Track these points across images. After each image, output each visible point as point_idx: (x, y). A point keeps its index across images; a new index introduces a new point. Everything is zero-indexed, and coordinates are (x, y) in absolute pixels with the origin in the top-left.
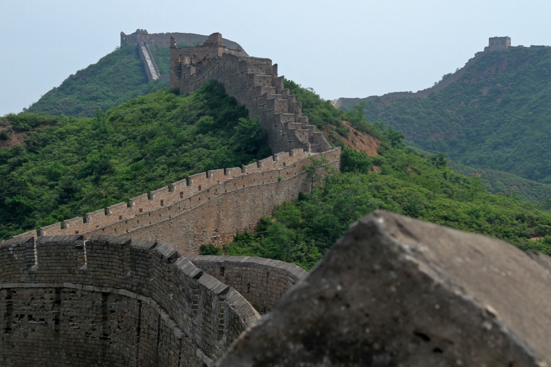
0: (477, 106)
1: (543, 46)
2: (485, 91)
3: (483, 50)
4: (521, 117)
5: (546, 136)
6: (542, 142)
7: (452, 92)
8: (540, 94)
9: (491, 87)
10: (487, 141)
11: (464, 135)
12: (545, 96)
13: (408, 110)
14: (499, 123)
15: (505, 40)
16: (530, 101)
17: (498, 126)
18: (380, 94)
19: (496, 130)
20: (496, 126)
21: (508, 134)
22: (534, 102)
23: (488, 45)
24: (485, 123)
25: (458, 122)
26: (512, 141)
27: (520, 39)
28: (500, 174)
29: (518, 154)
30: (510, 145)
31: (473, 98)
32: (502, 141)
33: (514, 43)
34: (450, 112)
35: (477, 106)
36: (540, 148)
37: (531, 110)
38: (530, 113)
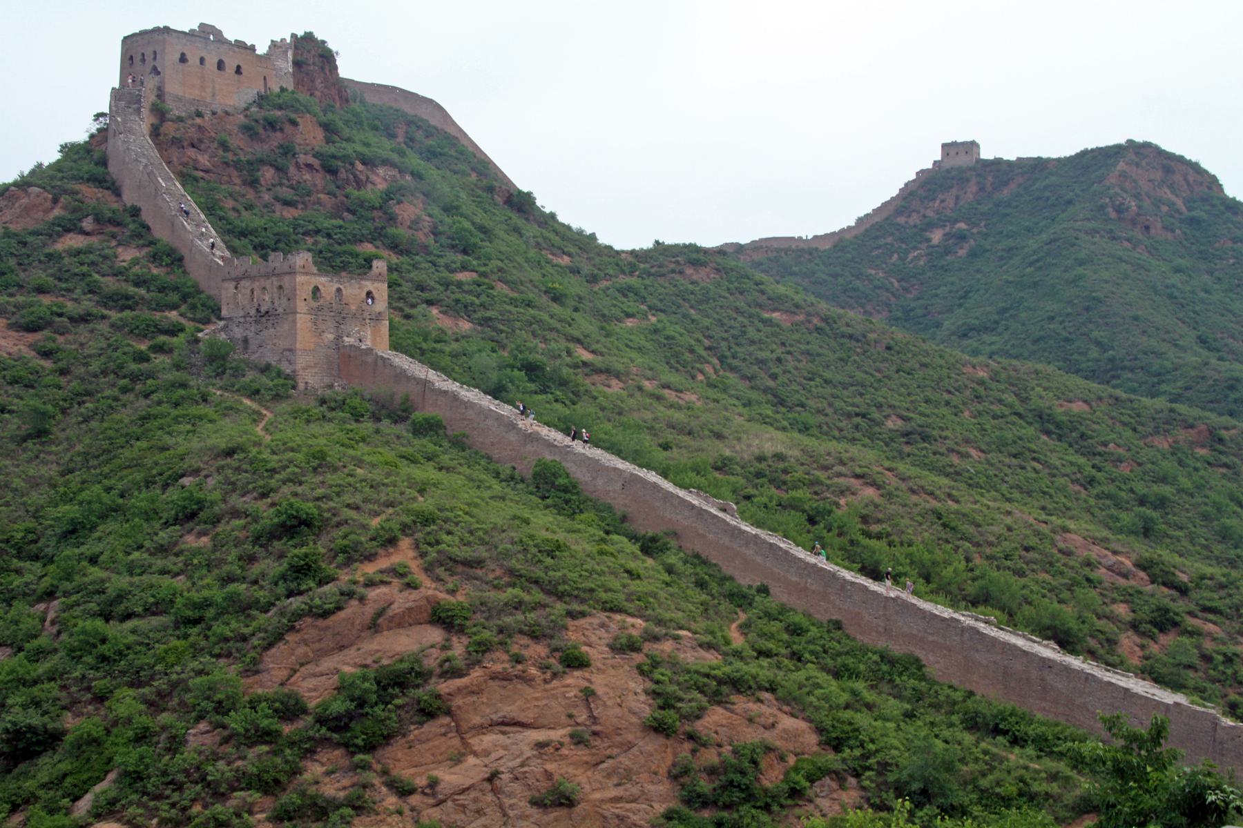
0: (922, 263)
1: (1039, 159)
2: (936, 236)
3: (930, 166)
4: (1011, 279)
5: (1069, 310)
6: (1061, 323)
7: (877, 237)
8: (1044, 236)
9: (947, 229)
10: (947, 324)
11: (899, 314)
12: (1056, 240)
13: (795, 269)
14: (967, 292)
15: (972, 146)
16: (1026, 250)
17: (965, 297)
18: (744, 240)
19: (960, 305)
20: (961, 298)
21: (988, 309)
22: (1035, 252)
23: (939, 158)
24: (939, 291)
25: (887, 290)
26: (997, 322)
27: (1001, 144)
28: (1037, 372)
29: (1013, 345)
30: (994, 330)
31: (915, 248)
32: (977, 322)
33: (986, 154)
34: (873, 272)
35: (922, 263)
36: (1059, 334)
37: (1031, 264)
38: (1029, 270)
